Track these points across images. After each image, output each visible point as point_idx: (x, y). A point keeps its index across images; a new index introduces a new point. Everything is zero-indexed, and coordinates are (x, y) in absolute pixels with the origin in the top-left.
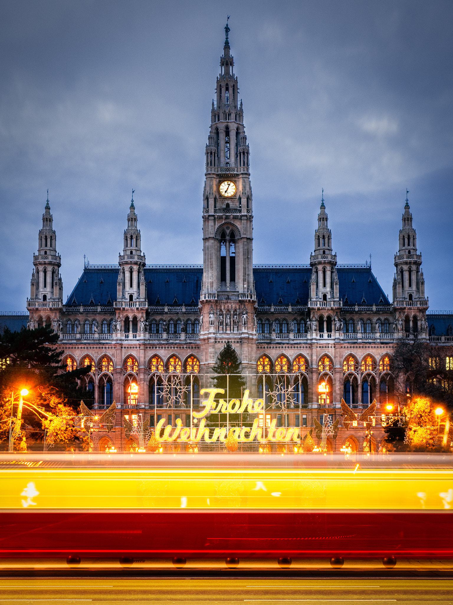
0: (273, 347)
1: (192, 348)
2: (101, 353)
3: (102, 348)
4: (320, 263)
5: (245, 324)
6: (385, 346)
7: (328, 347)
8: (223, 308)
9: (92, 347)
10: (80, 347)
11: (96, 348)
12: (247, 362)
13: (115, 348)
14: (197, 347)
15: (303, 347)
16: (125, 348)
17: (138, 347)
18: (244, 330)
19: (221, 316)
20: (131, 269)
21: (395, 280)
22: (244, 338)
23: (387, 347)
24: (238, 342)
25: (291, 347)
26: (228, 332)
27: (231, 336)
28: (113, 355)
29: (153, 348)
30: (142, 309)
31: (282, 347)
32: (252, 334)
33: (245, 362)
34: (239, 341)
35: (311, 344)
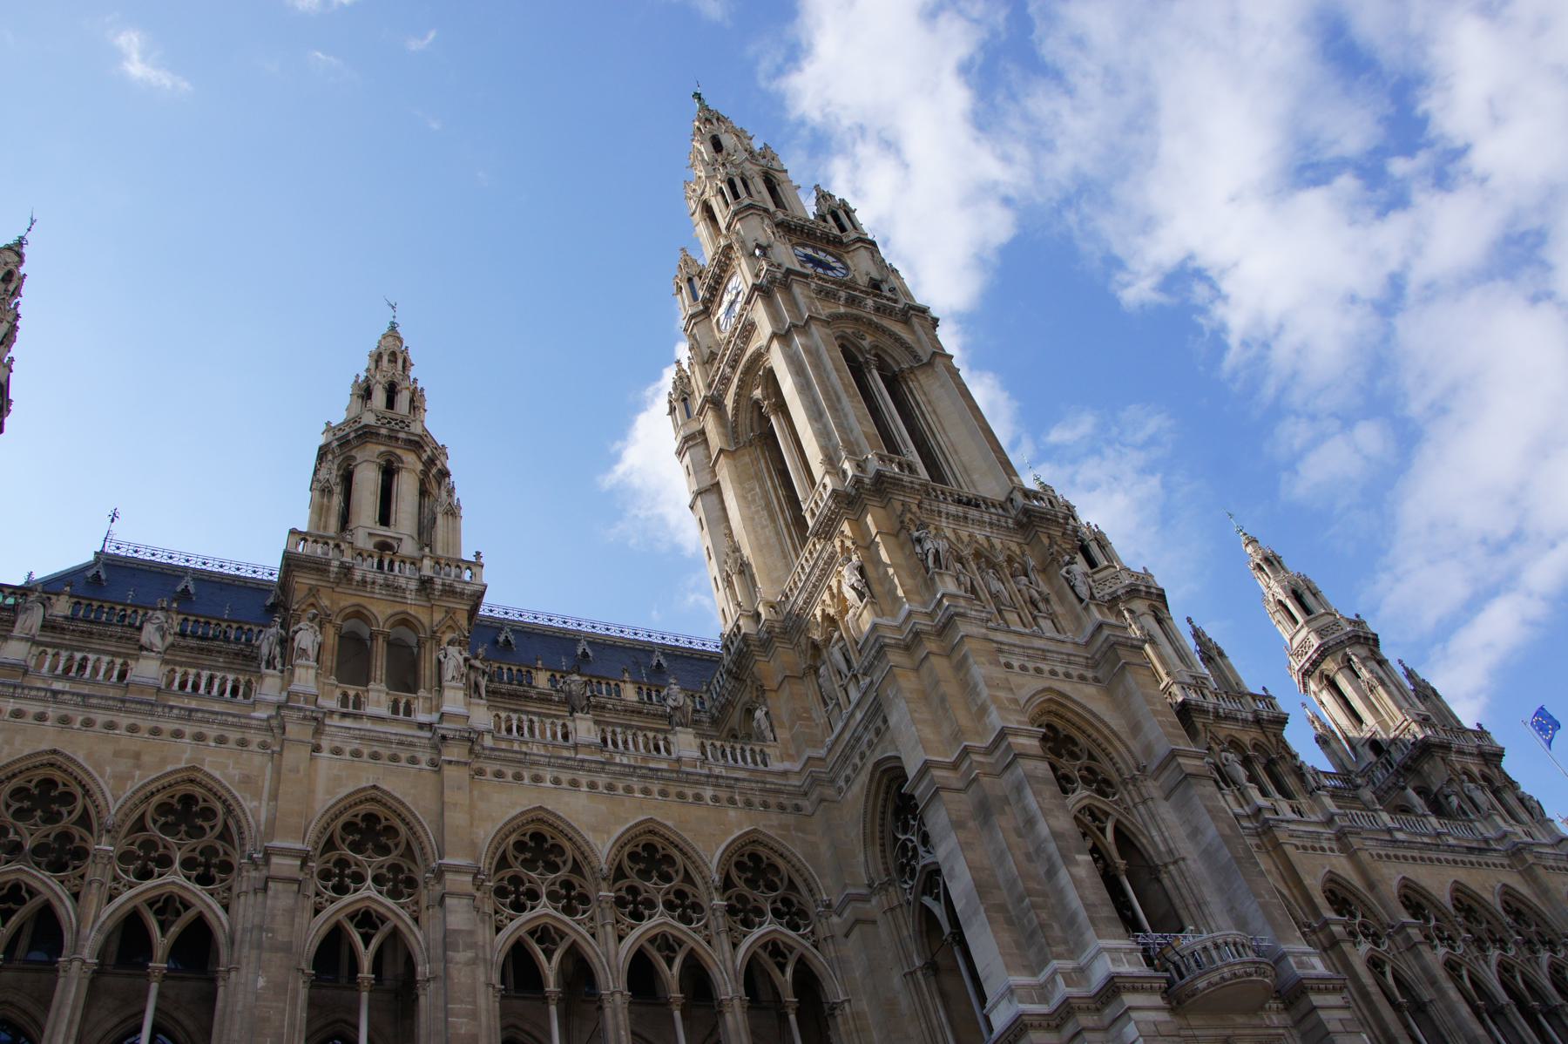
1: (749, 804)
2: (164, 761)
3: (178, 734)
4: (1133, 592)
9: (101, 717)
11: (133, 729)
13: (264, 745)
14: (772, 800)
16: (337, 751)
17: (424, 757)
20: (389, 462)
24: (1082, 678)
28: (246, 780)
29: (518, 777)
30: (449, 591)
34: (1089, 674)
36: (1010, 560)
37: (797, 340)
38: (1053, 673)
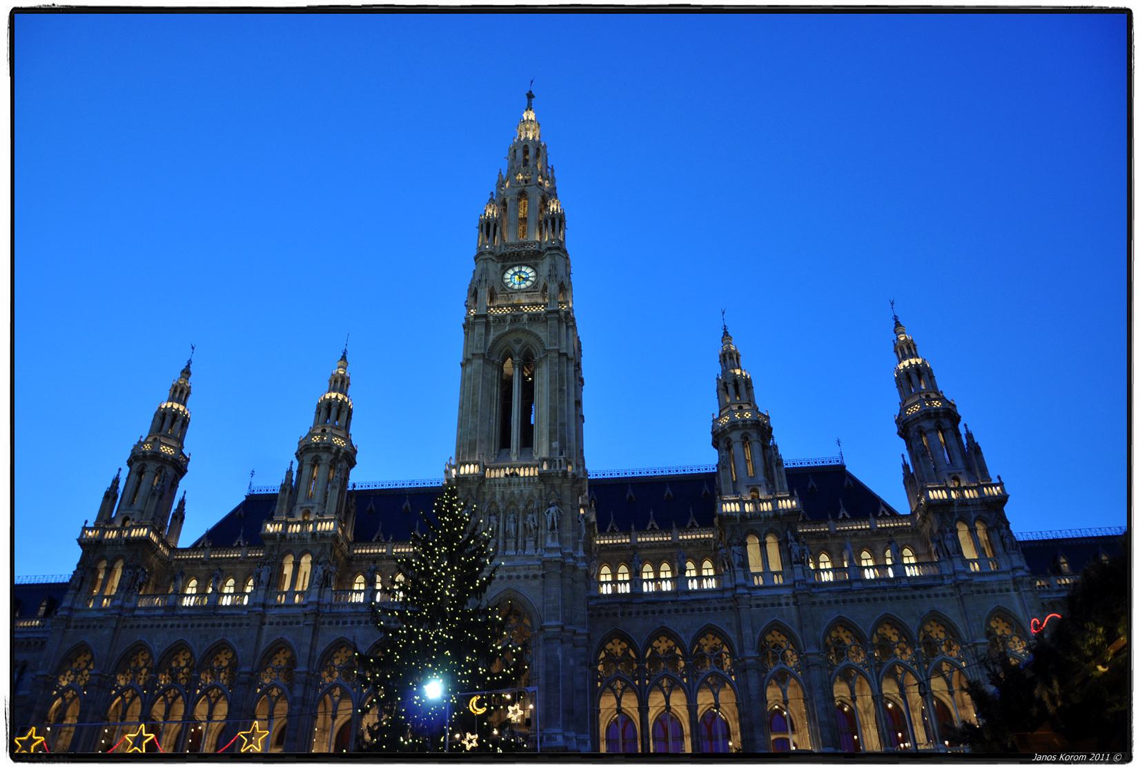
0: (638, 613)
3: (220, 625)
5: (553, 528)
6: (924, 593)
7: (780, 605)
8: (498, 496)
9: (196, 622)
10: (170, 623)
12: (560, 623)
15: (716, 609)
16: (271, 624)
18: (550, 543)
19: (493, 518)
21: (905, 467)
22: (549, 561)
23: (929, 596)
24: (535, 577)
25: (684, 611)
26: (511, 553)
27: (517, 561)
31: (661, 612)
32: (575, 558)
33: (554, 623)
35: (735, 599)
36: (531, 502)
37: (468, 370)
38: (518, 577)
